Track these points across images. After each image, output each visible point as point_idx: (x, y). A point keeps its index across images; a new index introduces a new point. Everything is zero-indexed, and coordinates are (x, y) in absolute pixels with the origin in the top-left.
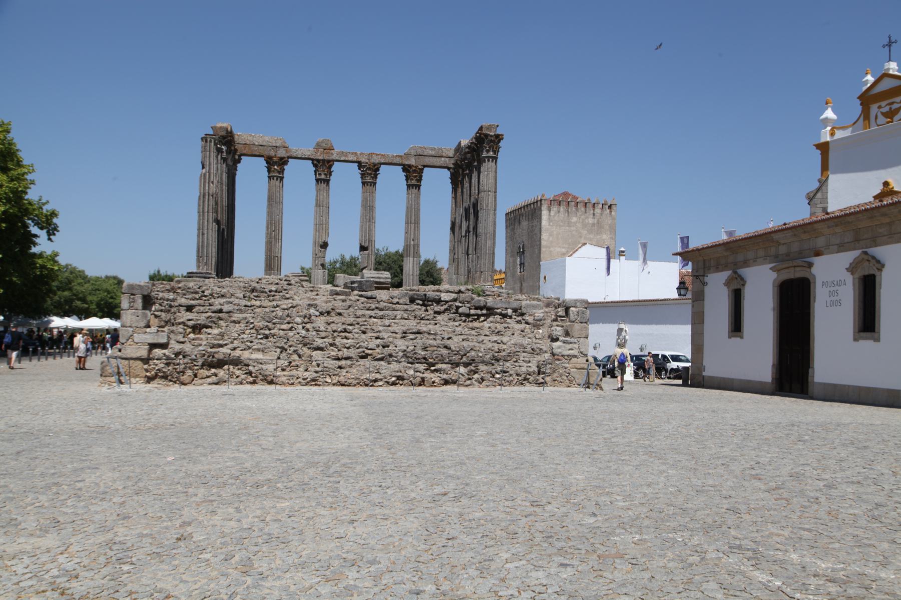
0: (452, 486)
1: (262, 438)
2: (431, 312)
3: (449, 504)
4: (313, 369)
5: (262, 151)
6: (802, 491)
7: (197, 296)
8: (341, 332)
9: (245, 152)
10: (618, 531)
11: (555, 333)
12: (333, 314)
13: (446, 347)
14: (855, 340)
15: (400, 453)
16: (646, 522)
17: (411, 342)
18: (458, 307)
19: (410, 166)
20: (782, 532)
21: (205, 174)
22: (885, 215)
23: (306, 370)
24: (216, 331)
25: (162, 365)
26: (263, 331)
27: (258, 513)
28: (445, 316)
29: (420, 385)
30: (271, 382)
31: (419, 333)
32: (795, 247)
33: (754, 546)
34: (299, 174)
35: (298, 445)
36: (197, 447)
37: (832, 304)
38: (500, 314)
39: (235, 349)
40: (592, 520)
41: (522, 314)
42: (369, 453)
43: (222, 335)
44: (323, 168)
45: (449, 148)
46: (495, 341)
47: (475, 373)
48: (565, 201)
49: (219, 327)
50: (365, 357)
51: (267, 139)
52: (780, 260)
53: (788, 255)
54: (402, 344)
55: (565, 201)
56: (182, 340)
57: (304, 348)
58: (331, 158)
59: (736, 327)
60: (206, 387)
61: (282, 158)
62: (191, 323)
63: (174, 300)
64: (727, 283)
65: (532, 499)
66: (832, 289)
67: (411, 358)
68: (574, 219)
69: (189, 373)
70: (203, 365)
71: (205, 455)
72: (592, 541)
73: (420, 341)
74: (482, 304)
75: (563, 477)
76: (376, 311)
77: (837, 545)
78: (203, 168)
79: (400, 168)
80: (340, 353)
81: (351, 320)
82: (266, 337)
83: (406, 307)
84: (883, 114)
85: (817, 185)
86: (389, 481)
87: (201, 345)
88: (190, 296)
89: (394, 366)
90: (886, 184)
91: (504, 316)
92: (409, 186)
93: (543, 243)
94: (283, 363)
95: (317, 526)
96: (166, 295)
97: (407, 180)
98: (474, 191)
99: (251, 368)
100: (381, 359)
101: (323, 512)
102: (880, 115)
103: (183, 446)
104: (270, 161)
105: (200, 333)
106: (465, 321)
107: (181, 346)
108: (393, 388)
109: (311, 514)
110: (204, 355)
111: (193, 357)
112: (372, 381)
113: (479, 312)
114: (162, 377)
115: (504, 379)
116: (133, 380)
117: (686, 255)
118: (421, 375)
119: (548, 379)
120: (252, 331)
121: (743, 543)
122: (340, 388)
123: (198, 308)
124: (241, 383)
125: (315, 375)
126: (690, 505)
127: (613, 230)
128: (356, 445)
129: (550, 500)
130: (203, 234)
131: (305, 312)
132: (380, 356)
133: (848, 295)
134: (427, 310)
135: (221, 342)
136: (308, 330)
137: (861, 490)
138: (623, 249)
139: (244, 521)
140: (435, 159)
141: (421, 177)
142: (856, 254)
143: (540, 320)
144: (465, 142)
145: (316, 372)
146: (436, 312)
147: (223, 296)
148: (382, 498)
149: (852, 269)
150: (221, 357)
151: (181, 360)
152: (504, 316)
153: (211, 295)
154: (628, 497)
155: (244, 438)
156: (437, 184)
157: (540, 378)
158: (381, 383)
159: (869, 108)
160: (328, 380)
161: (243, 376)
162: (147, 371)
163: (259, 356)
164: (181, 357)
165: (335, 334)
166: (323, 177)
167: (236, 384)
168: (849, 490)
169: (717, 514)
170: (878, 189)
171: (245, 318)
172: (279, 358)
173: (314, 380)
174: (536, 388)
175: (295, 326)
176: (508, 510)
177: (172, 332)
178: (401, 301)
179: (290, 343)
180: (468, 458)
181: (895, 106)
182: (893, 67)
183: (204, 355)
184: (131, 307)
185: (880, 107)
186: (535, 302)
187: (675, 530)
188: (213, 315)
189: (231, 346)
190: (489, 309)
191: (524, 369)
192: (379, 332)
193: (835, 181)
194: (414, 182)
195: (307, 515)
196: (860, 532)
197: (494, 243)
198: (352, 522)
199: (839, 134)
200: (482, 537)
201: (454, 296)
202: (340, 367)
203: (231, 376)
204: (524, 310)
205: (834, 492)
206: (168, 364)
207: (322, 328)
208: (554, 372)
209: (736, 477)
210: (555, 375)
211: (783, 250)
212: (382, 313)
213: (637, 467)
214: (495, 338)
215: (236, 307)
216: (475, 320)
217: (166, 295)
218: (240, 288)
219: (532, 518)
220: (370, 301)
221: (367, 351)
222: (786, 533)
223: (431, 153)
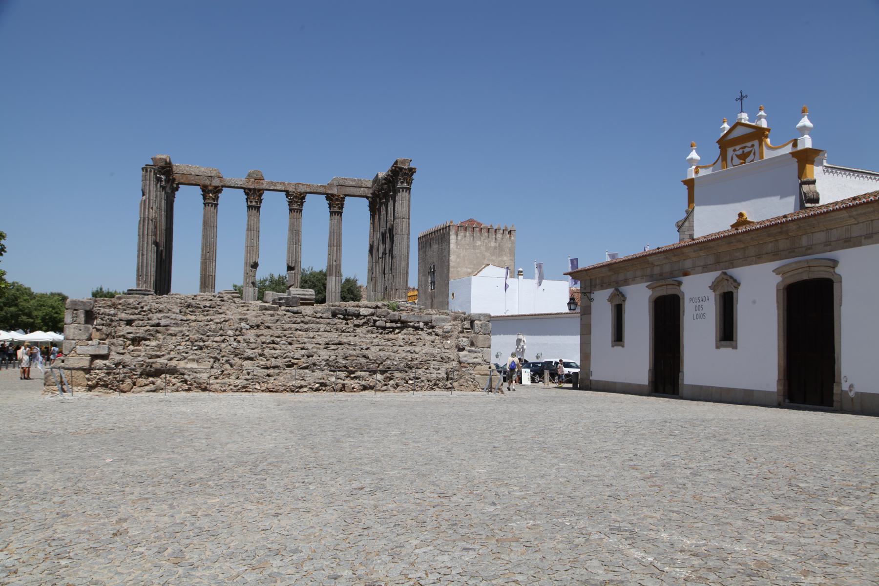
0: (368, 481)
1: (196, 440)
2: (351, 325)
3: (364, 497)
4: (243, 377)
5: (198, 180)
6: (672, 479)
7: (136, 311)
8: (269, 343)
9: (182, 181)
10: (514, 518)
11: (461, 343)
12: (262, 327)
13: (364, 356)
14: (718, 347)
15: (322, 452)
16: (540, 509)
17: (333, 352)
18: (375, 321)
19: (333, 195)
20: (655, 515)
21: (145, 201)
22: (740, 241)
23: (237, 378)
24: (154, 343)
25: (103, 375)
26: (197, 343)
27: (191, 508)
28: (364, 329)
29: (341, 391)
31: (340, 344)
32: (667, 268)
33: (631, 528)
34: (232, 203)
35: (229, 446)
36: (134, 449)
37: (699, 317)
38: (413, 327)
39: (171, 359)
40: (492, 509)
41: (433, 327)
42: (294, 453)
43: (159, 347)
44: (254, 196)
45: (368, 179)
46: (409, 351)
47: (391, 379)
48: (471, 227)
49: (157, 339)
50: (291, 366)
51: (203, 169)
52: (654, 279)
53: (661, 274)
54: (324, 354)
55: (471, 227)
56: (122, 351)
57: (236, 359)
58: (261, 187)
59: (618, 337)
61: (216, 187)
63: (115, 315)
64: (610, 300)
65: (439, 491)
66: (698, 304)
67: (333, 367)
68: (479, 243)
69: (129, 381)
70: (141, 374)
71: (142, 457)
72: (491, 527)
73: (341, 351)
75: (467, 471)
76: (302, 325)
77: (700, 525)
78: (143, 195)
79: (324, 196)
80: (268, 363)
81: (279, 332)
82: (201, 348)
83: (328, 321)
84: (737, 156)
85: (685, 215)
86: (312, 477)
87: (139, 356)
88: (130, 312)
89: (318, 374)
90: (741, 215)
91: (417, 328)
92: (332, 213)
93: (451, 264)
95: (244, 520)
96: (107, 311)
97: (330, 207)
98: (390, 217)
99: (186, 377)
101: (250, 506)
102: (734, 157)
103: (121, 449)
104: (205, 190)
105: (139, 345)
106: (381, 333)
107: (121, 357)
109: (240, 509)
110: (142, 365)
111: (133, 367)
112: (297, 387)
113: (394, 325)
114: (103, 386)
115: (416, 384)
116: (75, 388)
117: (575, 275)
118: (342, 382)
119: (455, 384)
120: (188, 343)
121: (621, 525)
122: (268, 394)
123: (137, 322)
124: (177, 391)
126: (577, 494)
127: (512, 253)
128: (281, 445)
129: (456, 492)
130: (143, 255)
131: (237, 325)
132: (304, 365)
133: (711, 309)
134: (347, 324)
135: (158, 353)
136: (239, 342)
137: (721, 476)
138: (521, 269)
139: (177, 516)
140: (355, 189)
141: (342, 205)
143: (448, 332)
144: (382, 174)
145: (247, 380)
146: (355, 326)
147: (160, 311)
148: (305, 493)
149: (714, 287)
150: (158, 366)
152: (417, 328)
153: (150, 310)
155: (179, 440)
156: (357, 211)
158: (305, 389)
159: (726, 151)
161: (179, 384)
162: (88, 380)
163: (194, 365)
164: (121, 367)
165: (264, 345)
166: (254, 204)
167: (172, 391)
168: (711, 476)
169: (600, 500)
170: (734, 219)
171: (181, 331)
172: (212, 367)
173: (244, 387)
174: (445, 393)
175: (227, 338)
176: (418, 501)
177: (113, 344)
178: (324, 316)
179: (223, 354)
180: (383, 456)
181: (747, 150)
182: (744, 117)
183: (142, 365)
184: (73, 322)
185: (735, 150)
186: (444, 316)
187: (564, 516)
188: (151, 328)
189: (168, 356)
190: (403, 322)
191: (434, 376)
192: (304, 343)
193: (700, 212)
194: (336, 209)
195: (236, 510)
196: (719, 513)
197: (408, 264)
198: (277, 515)
199: (703, 173)
200: (395, 526)
201: (372, 310)
202: (268, 375)
203: (168, 383)
204: (434, 323)
205: (699, 479)
206: (108, 374)
207: (252, 340)
208: (461, 378)
209: (617, 468)
210: (462, 381)
211: (657, 270)
212: (307, 326)
213: (532, 461)
215: (173, 322)
216: (391, 332)
217: (107, 311)
218: (176, 303)
219: (439, 508)
220: (296, 315)
221: (293, 361)
222: (658, 515)
223: (351, 183)
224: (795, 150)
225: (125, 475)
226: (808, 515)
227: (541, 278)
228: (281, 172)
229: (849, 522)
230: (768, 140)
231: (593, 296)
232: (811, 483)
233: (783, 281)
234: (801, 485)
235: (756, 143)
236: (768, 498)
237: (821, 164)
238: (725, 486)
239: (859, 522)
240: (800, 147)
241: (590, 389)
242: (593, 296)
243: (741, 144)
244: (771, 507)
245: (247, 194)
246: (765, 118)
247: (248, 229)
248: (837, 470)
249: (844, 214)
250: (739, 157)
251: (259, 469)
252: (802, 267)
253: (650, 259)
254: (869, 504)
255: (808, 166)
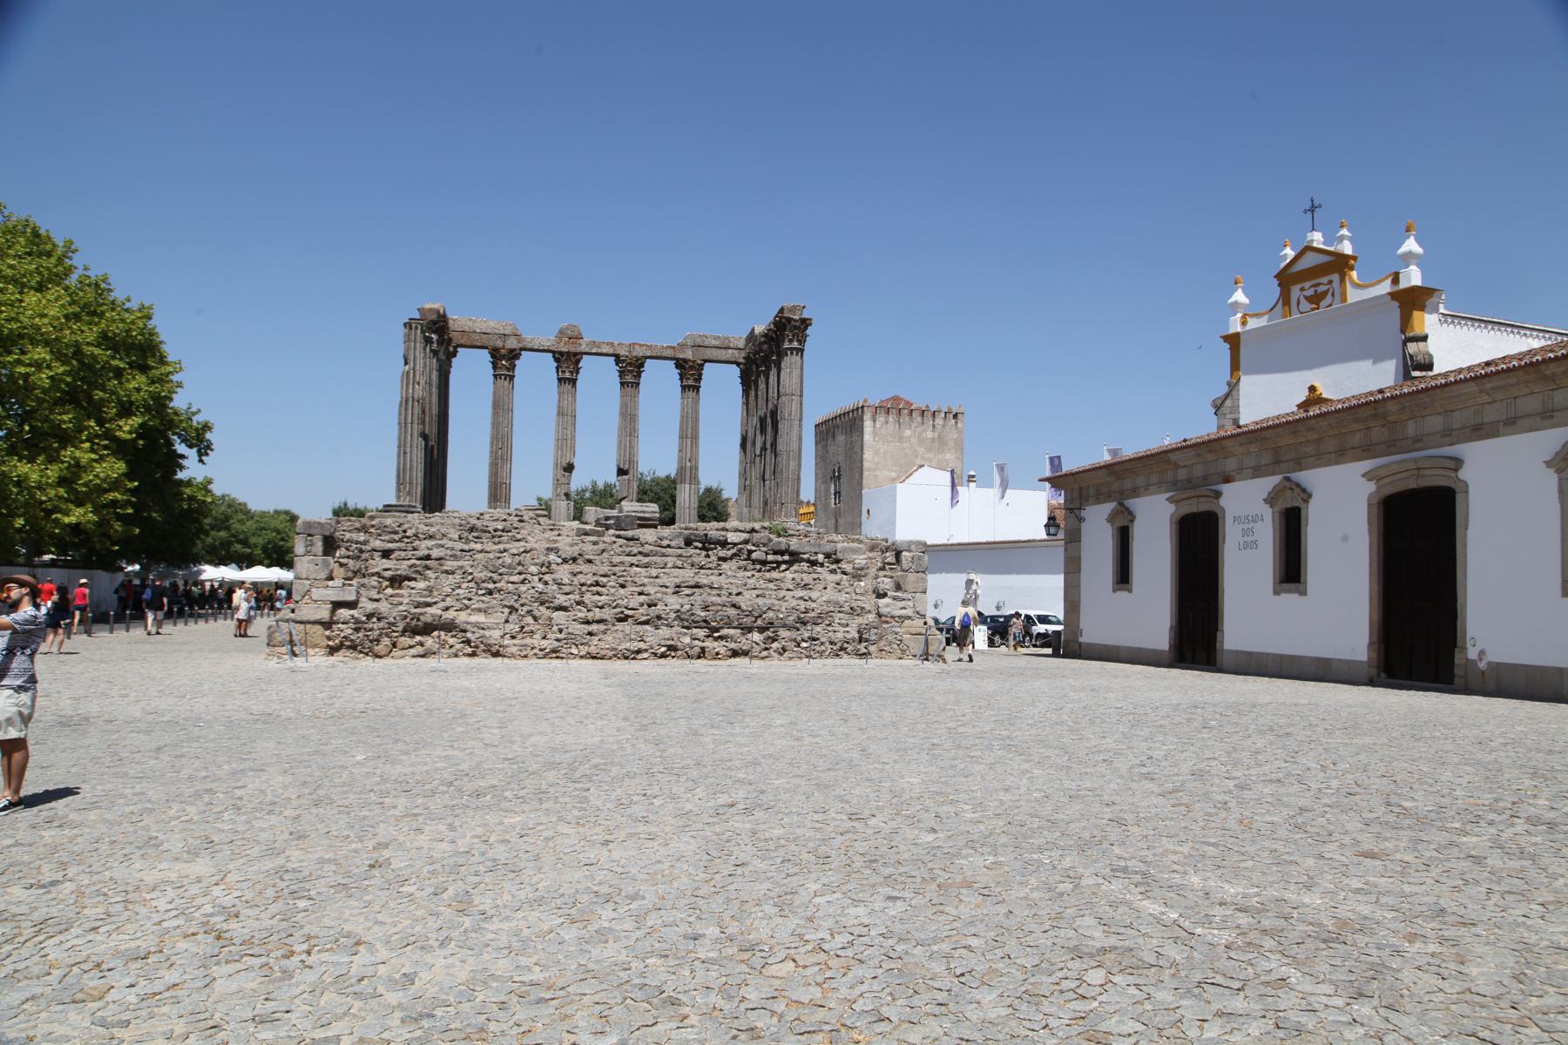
0: (742, 794)
2: (713, 558)
5: (485, 340)
7: (396, 537)
10: (964, 852)
11: (882, 586)
13: (734, 606)
14: (1276, 593)
15: (672, 750)
18: (750, 552)
19: (685, 360)
22: (1310, 429)
24: (422, 585)
27: (479, 831)
28: (733, 564)
29: (699, 657)
30: (496, 654)
31: (697, 586)
32: (1199, 471)
33: (1143, 868)
34: (536, 372)
35: (533, 739)
36: (397, 741)
37: (1247, 546)
38: (808, 561)
39: (447, 609)
40: (930, 838)
41: (838, 561)
43: (430, 590)
44: (568, 362)
45: (739, 336)
47: (774, 640)
48: (895, 408)
49: (426, 579)
52: (1179, 488)
53: (1189, 481)
54: (674, 602)
55: (895, 408)
59: (1123, 577)
60: (408, 660)
61: (512, 351)
62: (388, 574)
63: (365, 543)
66: (1246, 526)
67: (687, 621)
68: (908, 433)
69: (386, 641)
70: (404, 631)
71: (407, 753)
72: (930, 865)
73: (699, 597)
74: (783, 547)
77: (1250, 864)
78: (406, 363)
79: (672, 363)
80: (590, 615)
81: (606, 569)
82: (490, 593)
85: (1226, 389)
89: (664, 632)
90: (1312, 389)
91: (813, 563)
92: (684, 388)
93: (866, 464)
94: (513, 627)
96: (355, 536)
98: (773, 394)
99: (469, 635)
100: (646, 623)
102: (1303, 301)
104: (496, 354)
105: (400, 587)
107: (375, 605)
108: (662, 661)
109: (550, 833)
113: (779, 558)
114: (349, 647)
116: (310, 651)
119: (872, 648)
121: (1129, 864)
122: (590, 661)
123: (397, 554)
124: (456, 656)
125: (556, 644)
126: (1061, 816)
127: (959, 446)
133: (1266, 533)
136: (546, 583)
137: (1282, 790)
139: (460, 842)
142: (1275, 480)
144: (760, 329)
146: (720, 559)
149: (1271, 500)
150: (428, 619)
151: (374, 624)
152: (813, 563)
154: (979, 806)
155: (459, 729)
156: (723, 383)
157: (862, 648)
158: (645, 655)
159: (1289, 291)
160: (574, 651)
161: (459, 646)
162: (329, 638)
166: (567, 375)
168: (1266, 790)
169: (1096, 826)
170: (1302, 396)
173: (554, 651)
180: (764, 756)
181: (1321, 289)
182: (1317, 239)
184: (307, 553)
185: (1302, 289)
186: (855, 545)
187: (1041, 850)
189: (442, 605)
190: (792, 554)
191: (840, 635)
194: (690, 382)
195: (545, 834)
196: (1279, 846)
197: (799, 465)
198: (607, 843)
199: (1253, 323)
202: (590, 634)
203: (443, 644)
204: (840, 556)
205: (1247, 794)
206: (357, 630)
207: (566, 581)
209: (1122, 777)
210: (882, 643)
211: (1182, 474)
212: (647, 560)
213: (991, 766)
214: (800, 593)
217: (355, 536)
219: (850, 835)
222: (1185, 849)
223: (714, 342)
224: (1395, 289)
225: (384, 780)
226: (1416, 850)
227: (1004, 486)
228: (610, 327)
229: (1478, 860)
230: (1354, 274)
231: (1083, 513)
232: (1421, 802)
233: (1378, 488)
234: (1406, 804)
235: (1335, 277)
236: (1353, 824)
237: (1436, 310)
238: (1288, 806)
239: (1494, 861)
240: (1403, 285)
241: (1080, 657)
242: (1083, 513)
243: (1311, 280)
244: (1359, 838)
245: (557, 360)
246: (1350, 239)
247: (559, 414)
248: (1459, 781)
249: (1472, 387)
250: (1309, 299)
251: (578, 774)
252: (1407, 469)
253: (1173, 457)
254: (1509, 833)
255: (1415, 313)
